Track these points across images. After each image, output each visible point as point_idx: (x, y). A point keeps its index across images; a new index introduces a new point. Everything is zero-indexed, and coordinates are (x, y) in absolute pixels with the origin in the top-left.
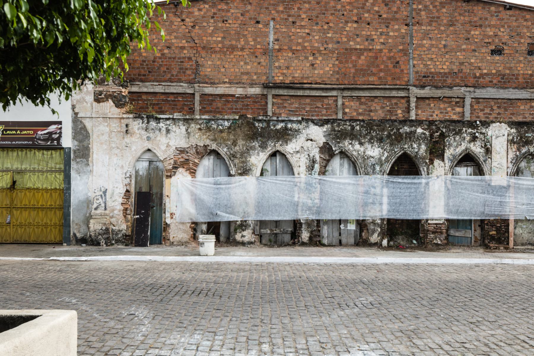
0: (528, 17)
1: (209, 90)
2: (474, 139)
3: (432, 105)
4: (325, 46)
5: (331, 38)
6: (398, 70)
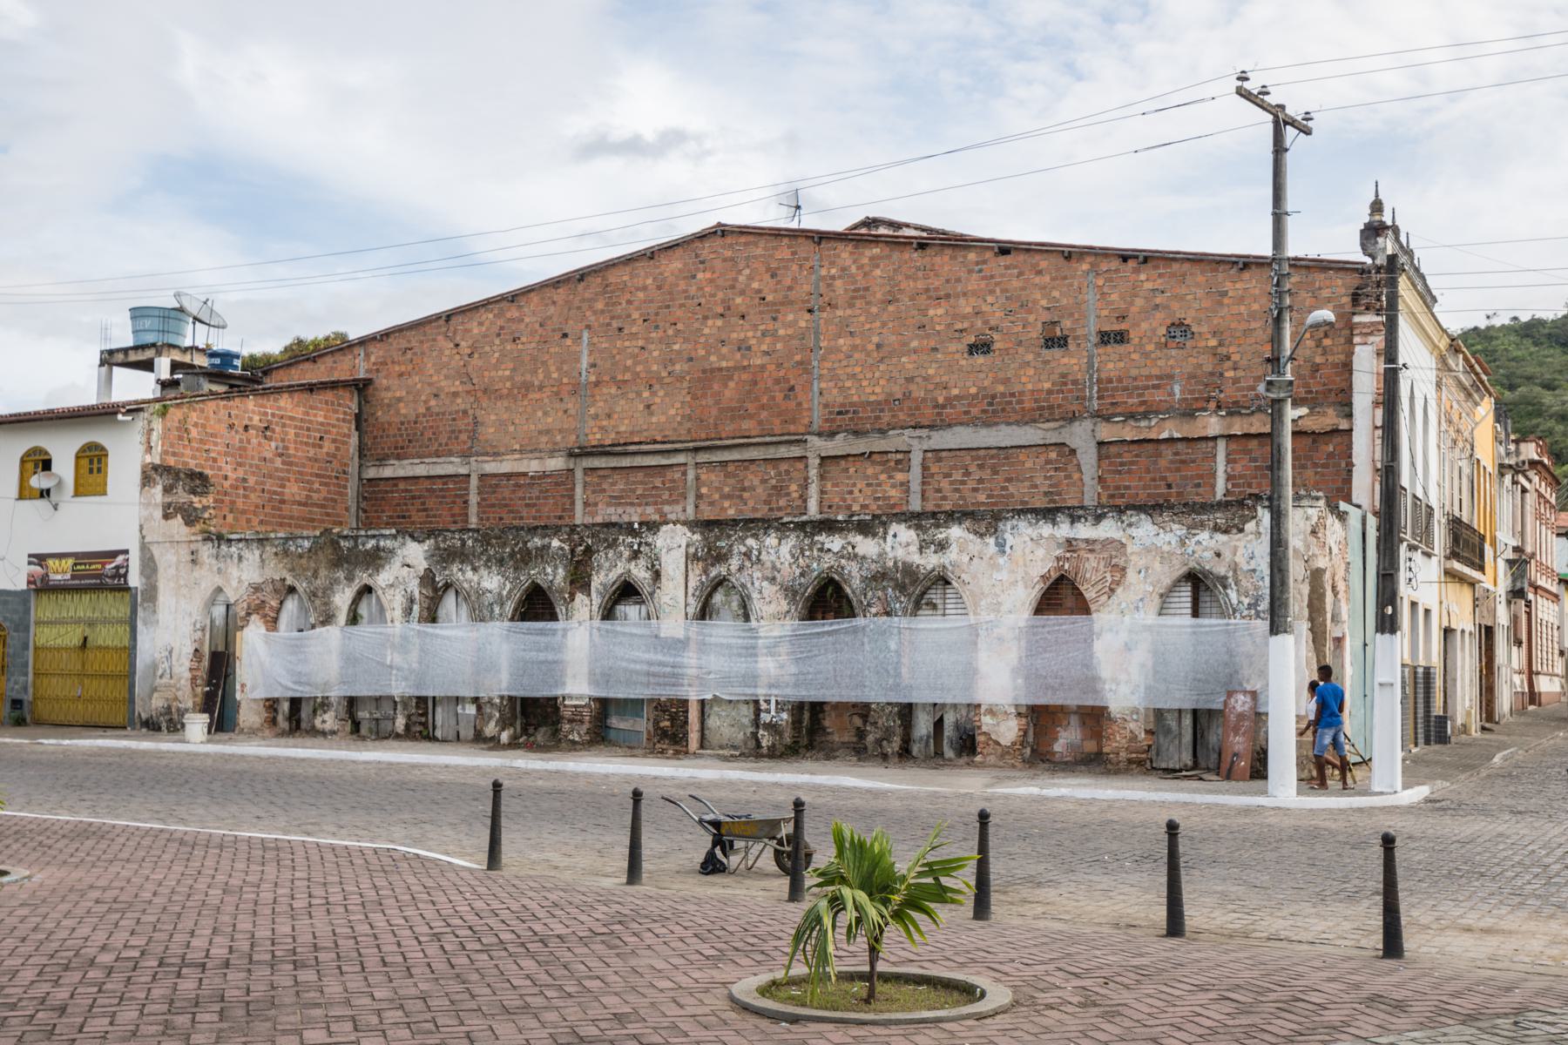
0: (1043, 264)
1: (491, 467)
2: (635, 555)
3: (852, 470)
4: (670, 369)
5: (679, 352)
6: (792, 404)
